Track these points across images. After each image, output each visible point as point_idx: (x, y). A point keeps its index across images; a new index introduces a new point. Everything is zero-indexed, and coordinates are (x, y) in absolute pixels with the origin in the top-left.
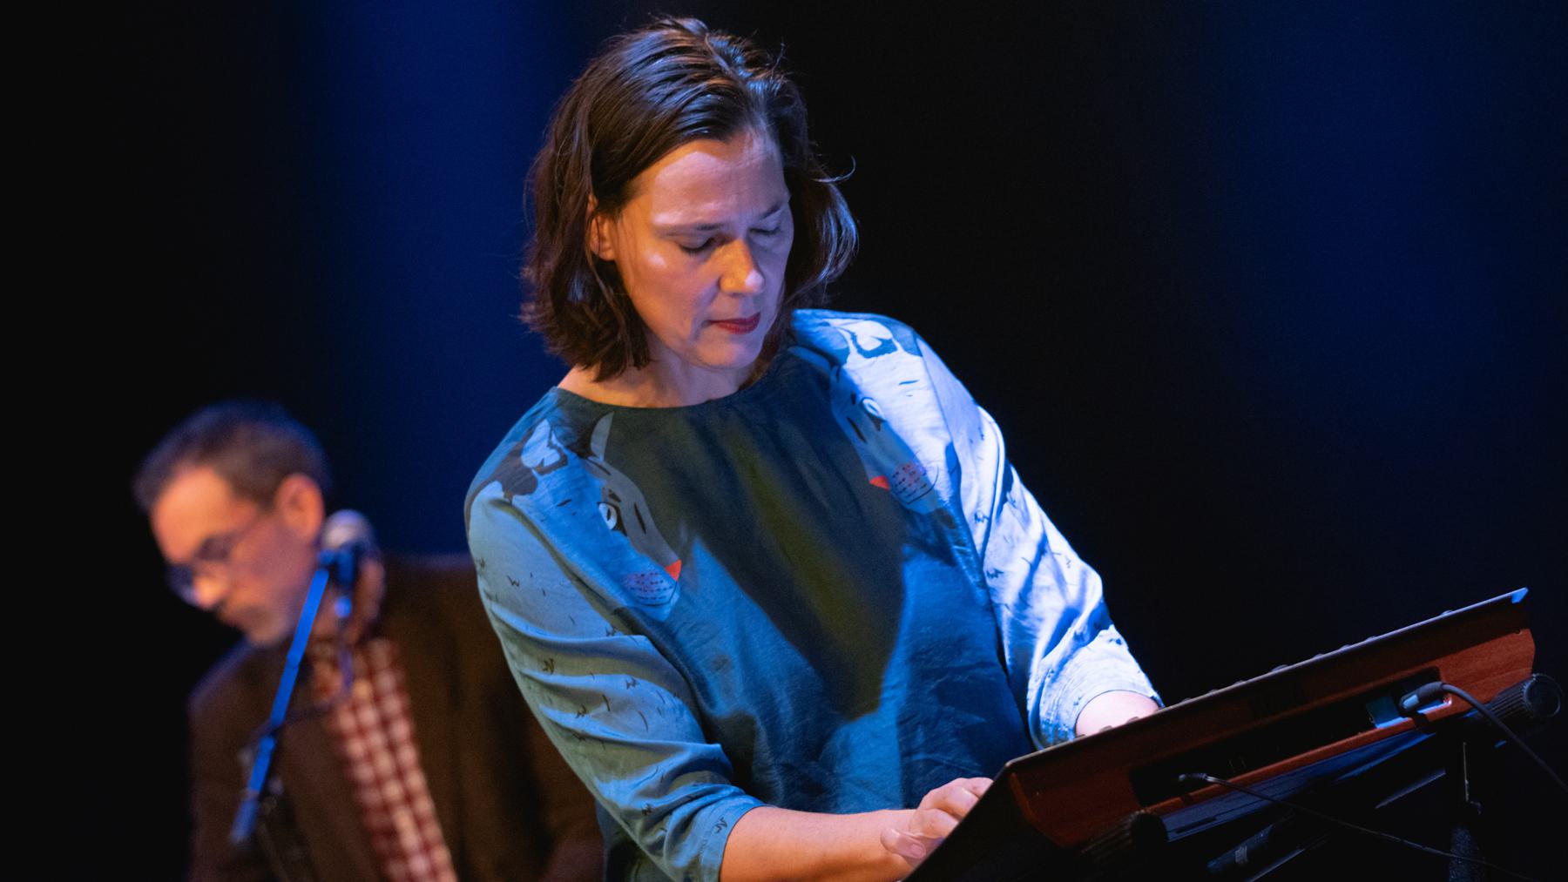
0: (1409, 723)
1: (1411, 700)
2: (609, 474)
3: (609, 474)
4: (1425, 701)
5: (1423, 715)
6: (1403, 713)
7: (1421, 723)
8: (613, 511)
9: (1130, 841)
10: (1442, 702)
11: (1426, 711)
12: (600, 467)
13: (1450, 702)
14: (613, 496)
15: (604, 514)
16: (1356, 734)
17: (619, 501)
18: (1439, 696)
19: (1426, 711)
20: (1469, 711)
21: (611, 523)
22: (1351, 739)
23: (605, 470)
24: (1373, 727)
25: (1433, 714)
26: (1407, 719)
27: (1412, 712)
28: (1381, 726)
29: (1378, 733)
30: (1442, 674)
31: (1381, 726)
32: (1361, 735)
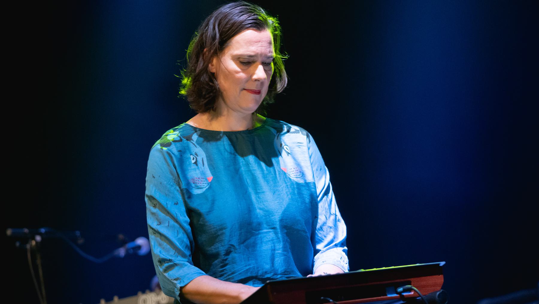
1: (400, 289)
2: (196, 147)
3: (196, 147)
4: (405, 291)
5: (403, 295)
6: (397, 293)
7: (402, 298)
8: (195, 158)
10: (410, 292)
11: (404, 294)
12: (194, 144)
13: (413, 293)
14: (196, 154)
15: (192, 158)
16: (381, 296)
17: (198, 156)
18: (410, 290)
19: (404, 294)
20: (418, 297)
21: (193, 161)
23: (195, 146)
24: (386, 295)
25: (406, 295)
26: (398, 295)
27: (400, 293)
28: (389, 296)
29: (386, 298)
30: (412, 283)
31: (389, 296)
32: (382, 297)
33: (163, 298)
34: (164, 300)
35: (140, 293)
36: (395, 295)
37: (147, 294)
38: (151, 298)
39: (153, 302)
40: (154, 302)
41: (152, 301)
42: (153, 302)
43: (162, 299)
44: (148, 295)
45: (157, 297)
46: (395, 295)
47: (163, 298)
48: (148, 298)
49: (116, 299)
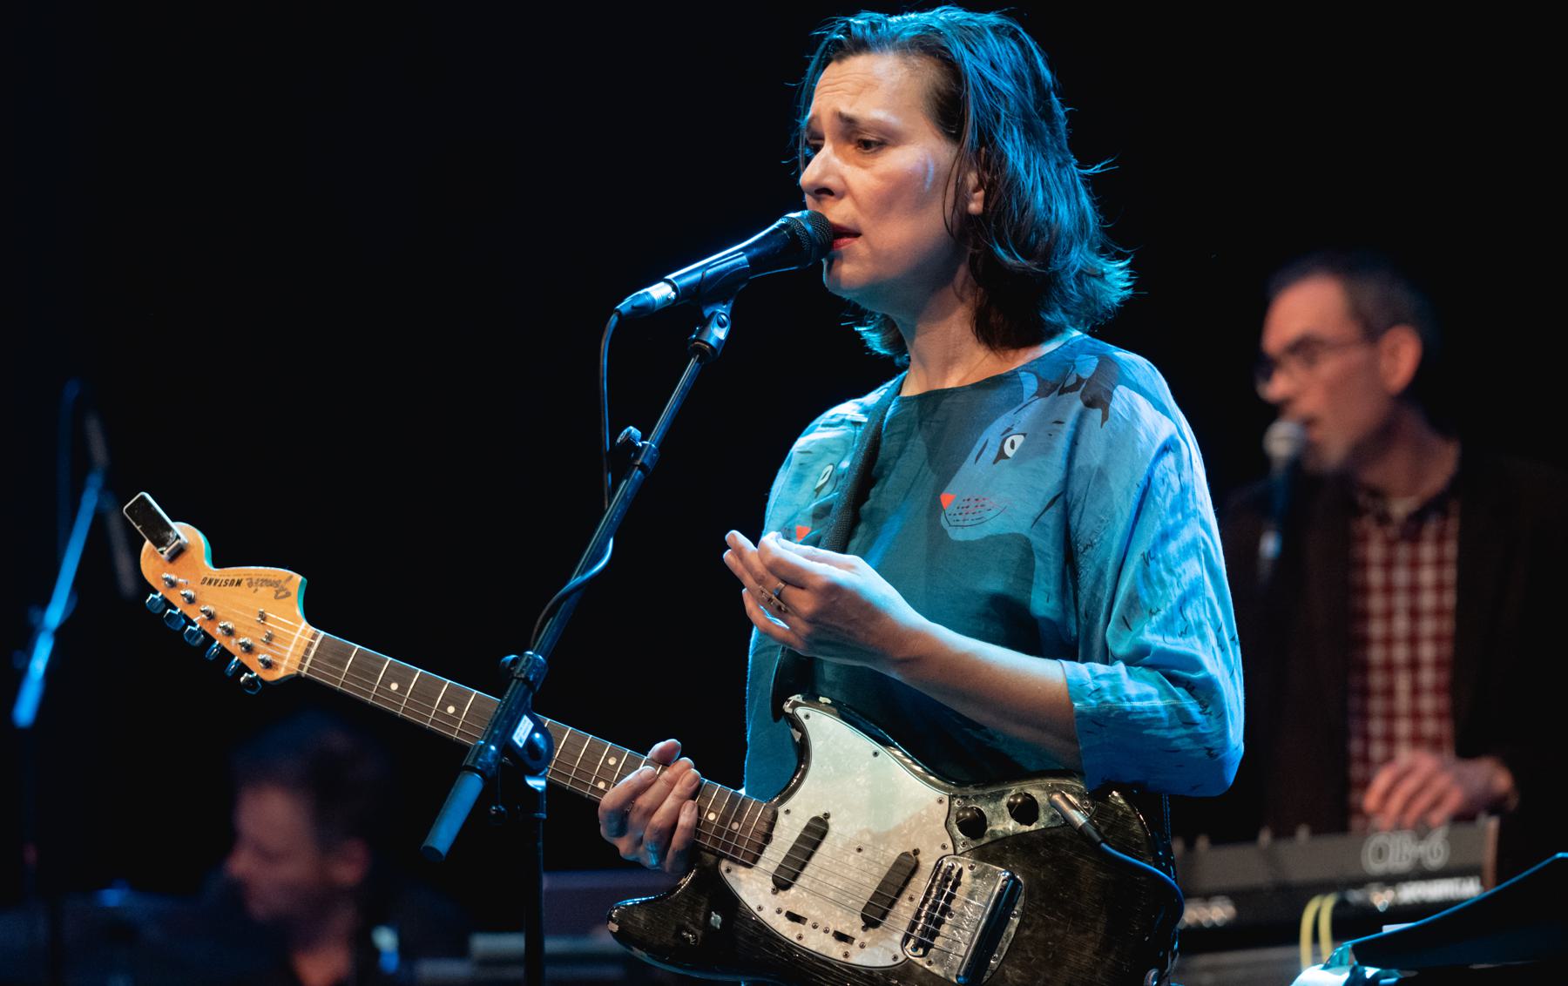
34: (1435, 855)
39: (1404, 858)
40: (1407, 857)
42: (1404, 858)
45: (1418, 845)
48: (1391, 846)
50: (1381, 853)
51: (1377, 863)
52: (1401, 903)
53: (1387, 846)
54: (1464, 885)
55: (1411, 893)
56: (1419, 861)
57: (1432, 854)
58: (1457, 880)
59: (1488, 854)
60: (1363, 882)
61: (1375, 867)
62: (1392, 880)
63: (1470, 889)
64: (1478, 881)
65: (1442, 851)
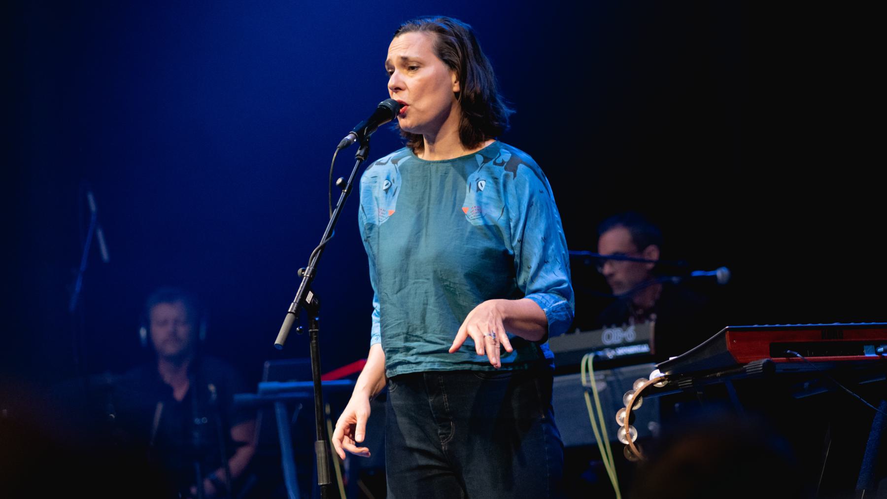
0: (877, 357)
1: (881, 350)
5: (884, 356)
6: (877, 353)
9: (762, 371)
22: (855, 356)
24: (864, 354)
26: (877, 356)
28: (867, 355)
29: (864, 357)
33: (630, 335)
35: (605, 327)
36: (874, 355)
37: (612, 328)
38: (617, 334)
39: (618, 338)
40: (619, 338)
41: (617, 337)
42: (618, 338)
43: (629, 336)
44: (613, 330)
45: (623, 333)
46: (874, 355)
47: (630, 335)
48: (613, 333)
49: (578, 331)
50: (609, 337)
51: (606, 340)
52: (617, 355)
53: (611, 334)
54: (642, 347)
55: (621, 351)
56: (624, 339)
57: (629, 336)
58: (639, 346)
59: (651, 335)
60: (603, 348)
61: (607, 342)
62: (614, 347)
63: (645, 349)
64: (647, 345)
65: (633, 336)
